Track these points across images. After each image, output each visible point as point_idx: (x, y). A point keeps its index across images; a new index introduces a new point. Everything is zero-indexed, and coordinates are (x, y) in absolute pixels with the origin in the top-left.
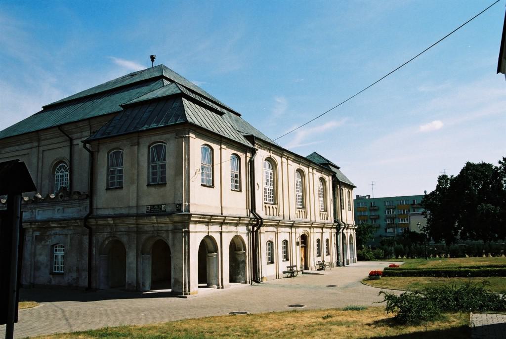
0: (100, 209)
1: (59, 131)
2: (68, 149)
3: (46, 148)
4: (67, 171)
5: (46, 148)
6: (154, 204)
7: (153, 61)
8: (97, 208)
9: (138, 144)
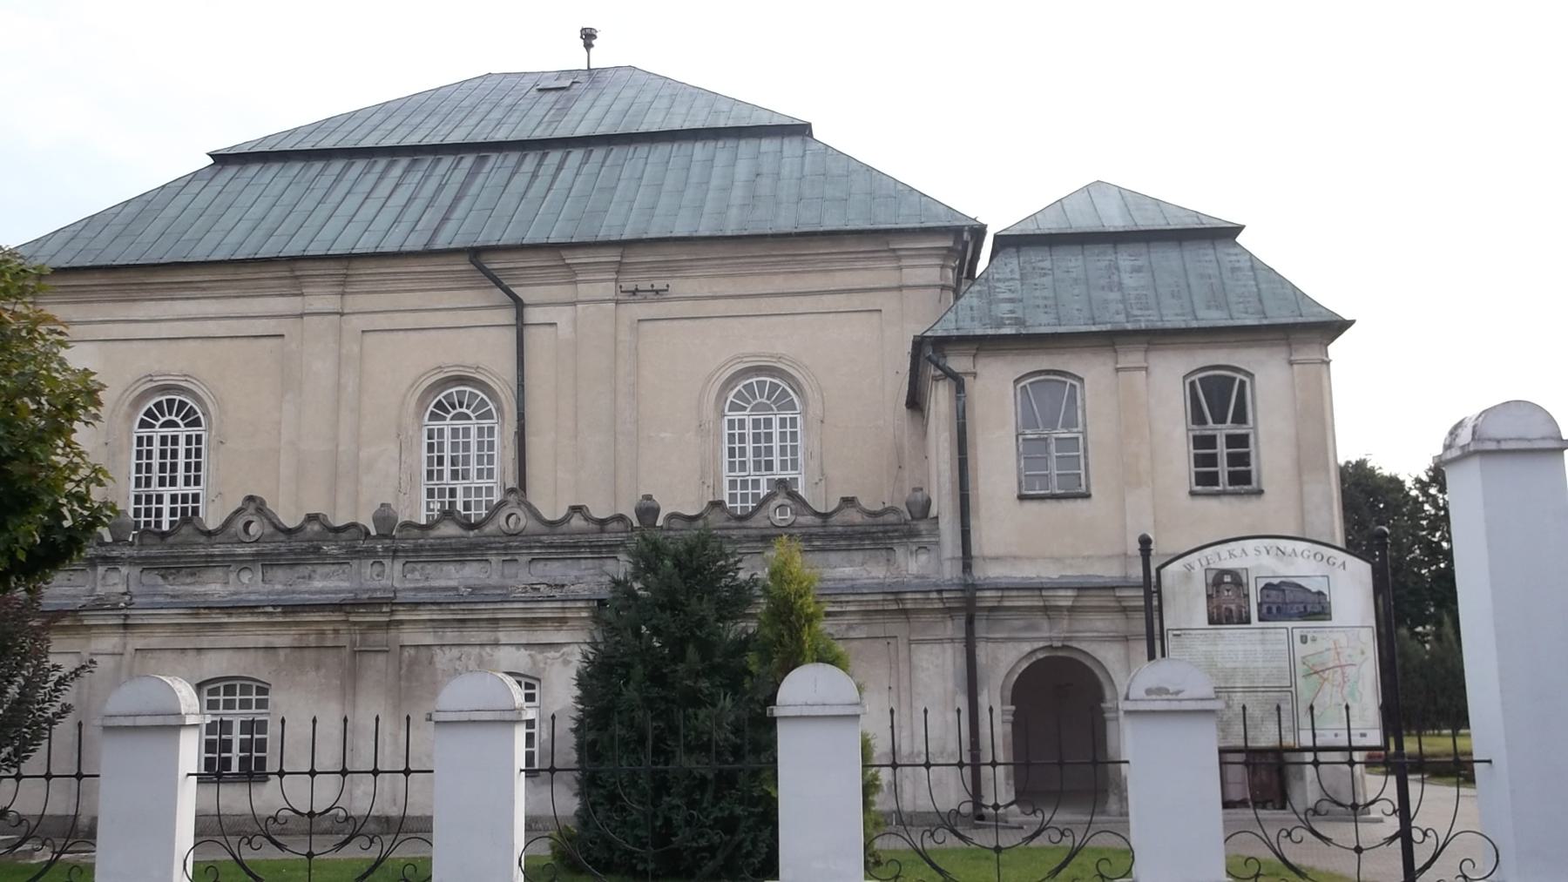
0: (997, 558)
1: (472, 267)
3: (381, 321)
4: (488, 415)
5: (381, 321)
7: (588, 46)
8: (984, 558)
9: (1146, 369)
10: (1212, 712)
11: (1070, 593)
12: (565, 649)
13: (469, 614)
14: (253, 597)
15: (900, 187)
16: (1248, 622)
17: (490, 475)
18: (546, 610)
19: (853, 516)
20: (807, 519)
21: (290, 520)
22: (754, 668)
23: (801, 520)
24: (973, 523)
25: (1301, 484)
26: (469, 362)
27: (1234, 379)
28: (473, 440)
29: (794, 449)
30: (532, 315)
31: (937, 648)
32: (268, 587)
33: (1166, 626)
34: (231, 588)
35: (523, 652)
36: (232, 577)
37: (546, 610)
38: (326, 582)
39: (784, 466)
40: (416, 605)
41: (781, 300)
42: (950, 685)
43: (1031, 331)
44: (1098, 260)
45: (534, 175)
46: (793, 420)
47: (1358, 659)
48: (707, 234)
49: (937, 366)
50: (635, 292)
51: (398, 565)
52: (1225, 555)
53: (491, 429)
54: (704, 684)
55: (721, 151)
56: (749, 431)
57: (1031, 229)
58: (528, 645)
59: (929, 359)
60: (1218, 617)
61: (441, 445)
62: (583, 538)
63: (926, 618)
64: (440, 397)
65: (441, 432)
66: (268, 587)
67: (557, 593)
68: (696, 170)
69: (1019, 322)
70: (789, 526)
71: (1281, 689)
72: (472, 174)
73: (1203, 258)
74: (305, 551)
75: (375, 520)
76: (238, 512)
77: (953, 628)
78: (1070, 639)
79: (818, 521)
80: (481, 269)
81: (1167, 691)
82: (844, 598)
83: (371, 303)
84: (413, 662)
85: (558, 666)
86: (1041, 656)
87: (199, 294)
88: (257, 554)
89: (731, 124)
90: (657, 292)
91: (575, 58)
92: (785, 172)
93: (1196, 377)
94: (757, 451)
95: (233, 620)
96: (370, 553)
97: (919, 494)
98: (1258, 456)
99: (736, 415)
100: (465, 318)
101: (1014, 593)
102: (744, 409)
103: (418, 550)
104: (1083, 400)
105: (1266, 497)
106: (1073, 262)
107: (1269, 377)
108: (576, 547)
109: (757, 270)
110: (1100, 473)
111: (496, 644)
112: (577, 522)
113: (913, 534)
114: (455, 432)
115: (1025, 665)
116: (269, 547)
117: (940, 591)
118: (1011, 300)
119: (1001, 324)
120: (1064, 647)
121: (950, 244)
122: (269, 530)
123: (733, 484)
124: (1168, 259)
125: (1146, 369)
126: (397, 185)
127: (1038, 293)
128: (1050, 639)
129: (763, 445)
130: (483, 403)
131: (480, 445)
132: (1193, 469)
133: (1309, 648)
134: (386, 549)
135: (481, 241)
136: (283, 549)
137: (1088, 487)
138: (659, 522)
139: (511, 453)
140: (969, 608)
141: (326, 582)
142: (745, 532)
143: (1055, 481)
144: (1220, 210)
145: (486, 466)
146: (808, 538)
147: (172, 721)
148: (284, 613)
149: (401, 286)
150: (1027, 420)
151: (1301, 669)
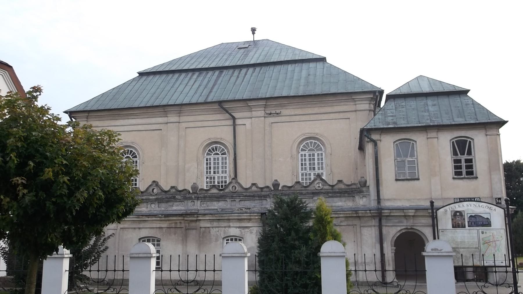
0: (388, 200)
2: (232, 127)
6: (464, 197)
7: (253, 33)
8: (384, 200)
9: (437, 138)
10: (452, 256)
11: (413, 211)
12: (251, 228)
13: (220, 217)
14: (155, 212)
15: (355, 78)
16: (465, 227)
17: (226, 173)
18: (245, 216)
19: (342, 186)
20: (327, 187)
21: (166, 189)
22: (312, 238)
23: (325, 187)
24: (381, 188)
25: (491, 175)
26: (218, 137)
27: (467, 141)
28: (220, 161)
29: (322, 163)
30: (238, 122)
31: (369, 229)
32: (159, 209)
33: (439, 228)
34: (149, 209)
35: (238, 229)
36: (149, 206)
37: (245, 216)
38: (177, 207)
39: (319, 169)
40: (205, 215)
41: (317, 115)
42: (374, 240)
43: (399, 126)
44: (421, 102)
45: (238, 77)
46: (322, 154)
47: (500, 239)
48: (293, 95)
49: (368, 138)
50: (270, 114)
51: (199, 202)
52: (457, 206)
53: (226, 158)
54: (297, 243)
55: (297, 67)
56: (307, 158)
57: (398, 92)
58: (239, 227)
59: (365, 136)
60: (456, 226)
61: (210, 163)
62: (256, 194)
63: (366, 219)
64: (210, 148)
65: (210, 159)
66: (159, 209)
67: (248, 211)
68: (289, 74)
69: (395, 123)
70: (321, 189)
71: (476, 248)
72: (218, 77)
73: (456, 100)
74: (171, 198)
75: (192, 188)
76: (150, 186)
77: (375, 222)
78: (413, 226)
79: (330, 188)
80: (222, 108)
81: (438, 250)
82: (339, 213)
83: (188, 119)
84: (204, 232)
85: (249, 234)
86: (404, 231)
87: (136, 117)
88: (157, 199)
89: (300, 58)
90: (277, 114)
91: (249, 37)
92: (318, 74)
93: (454, 140)
94: (310, 164)
95: (150, 219)
96: (190, 198)
97: (363, 179)
98: (476, 166)
99: (303, 153)
100: (217, 123)
101: (394, 211)
102: (306, 150)
103: (205, 197)
104: (416, 148)
105: (478, 179)
106: (412, 103)
107: (479, 140)
108: (254, 196)
109: (309, 106)
110: (422, 171)
111: (229, 227)
112: (254, 188)
113: (361, 192)
114: (214, 159)
115: (398, 234)
116: (160, 197)
117: (370, 210)
118: (392, 116)
119: (389, 124)
120: (411, 229)
121: (372, 96)
122: (160, 191)
123: (302, 175)
124: (444, 101)
125: (437, 138)
126: (195, 81)
127: (401, 114)
128: (407, 226)
129: (312, 162)
130: (223, 150)
131: (222, 163)
132: (454, 170)
133: (484, 235)
134: (195, 197)
135: (222, 99)
136: (164, 197)
137: (418, 176)
138: (280, 188)
139: (232, 166)
140: (380, 216)
141: (177, 207)
142: (307, 191)
143: (408, 175)
144: (462, 85)
145: (224, 170)
146: (328, 193)
147: (149, 255)
148: (165, 217)
149: (197, 113)
150: (398, 155)
151: (482, 242)
